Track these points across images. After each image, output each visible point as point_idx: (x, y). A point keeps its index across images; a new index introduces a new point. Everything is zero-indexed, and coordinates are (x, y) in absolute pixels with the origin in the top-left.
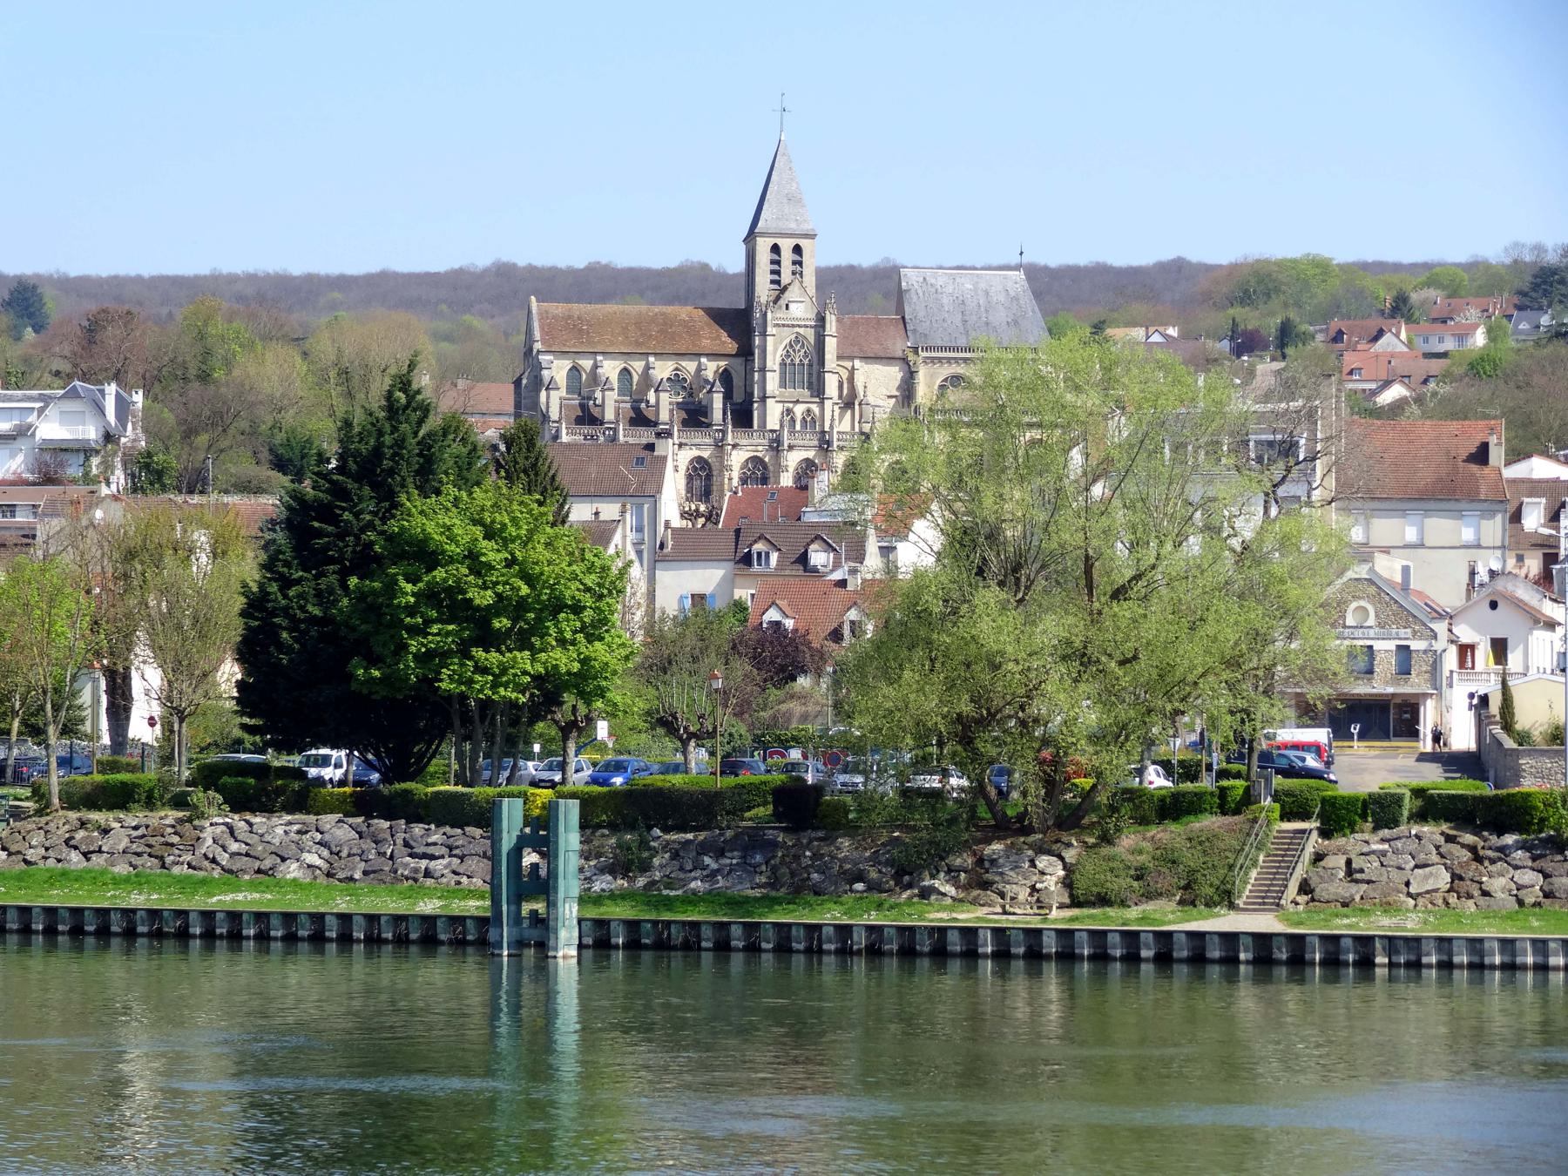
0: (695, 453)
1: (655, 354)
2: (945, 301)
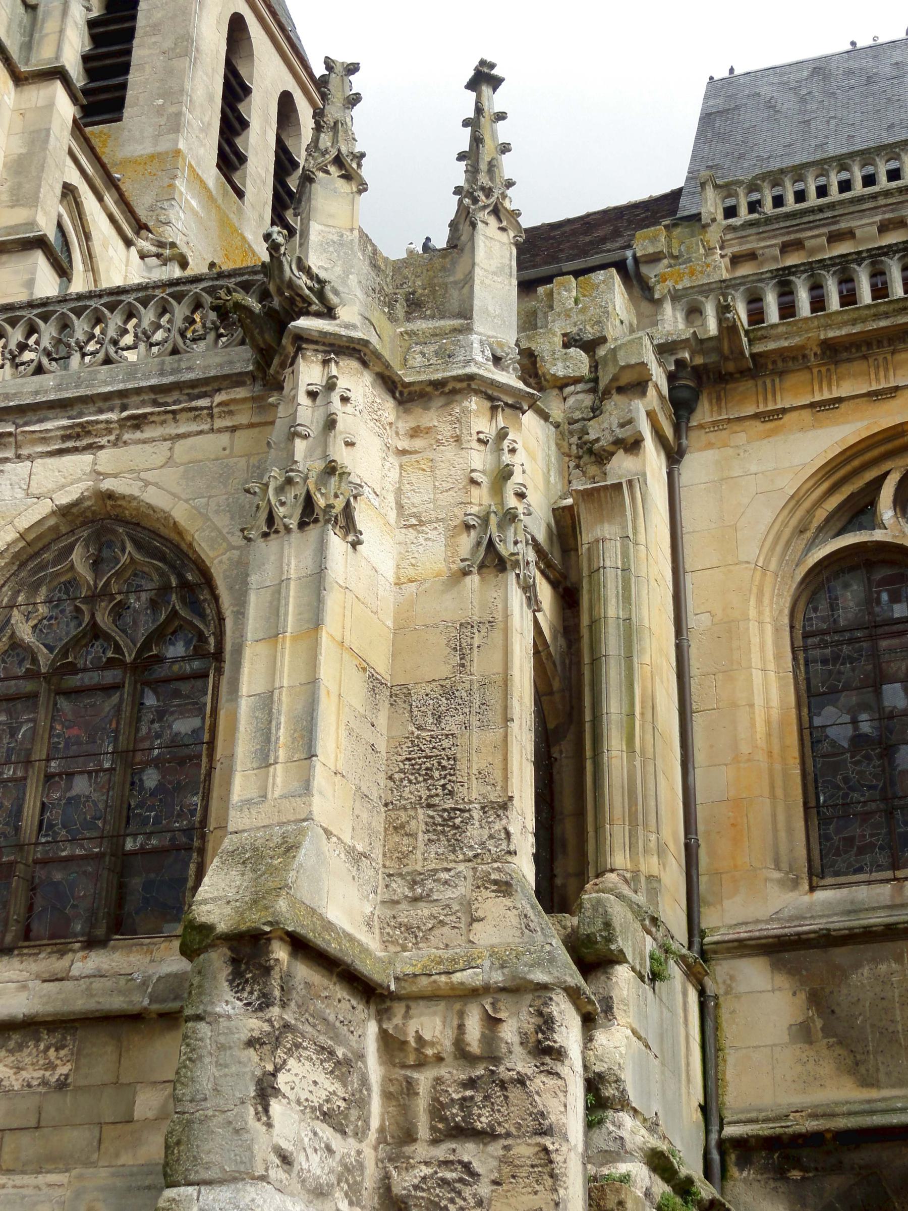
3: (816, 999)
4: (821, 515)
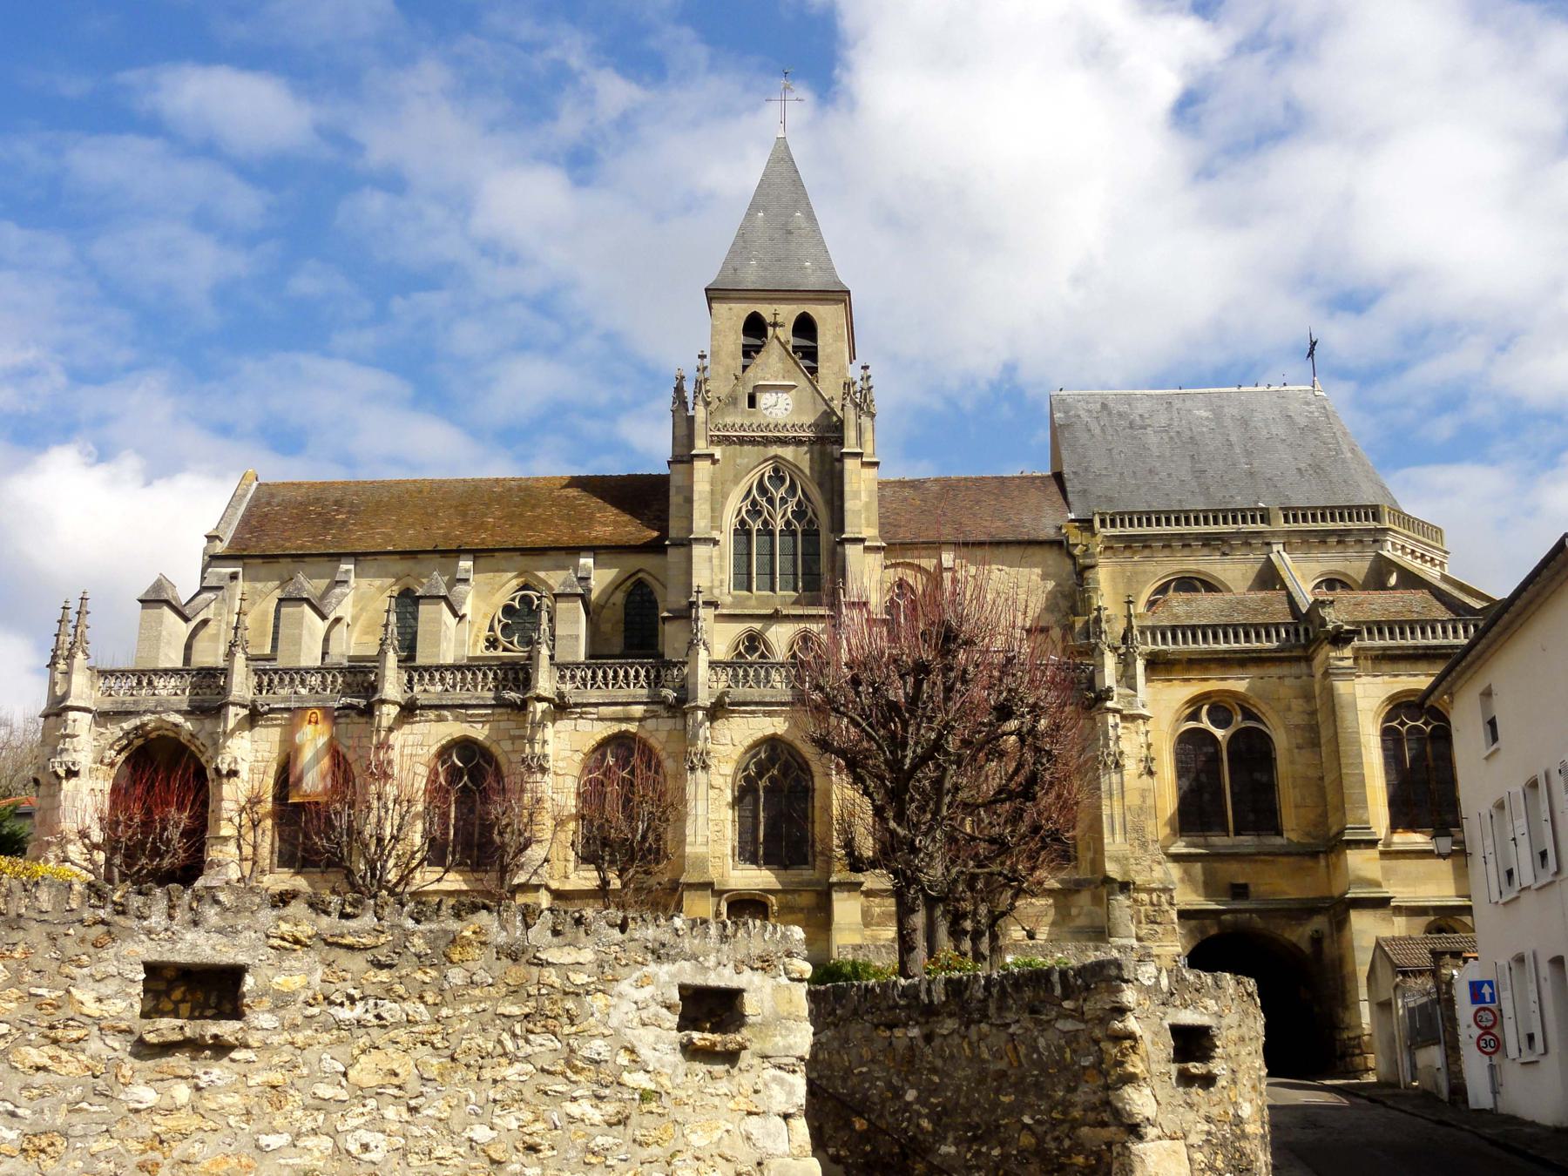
0: (453, 729)
1: (476, 554)
2: (1152, 439)
3: (1186, 872)
4: (1183, 715)
